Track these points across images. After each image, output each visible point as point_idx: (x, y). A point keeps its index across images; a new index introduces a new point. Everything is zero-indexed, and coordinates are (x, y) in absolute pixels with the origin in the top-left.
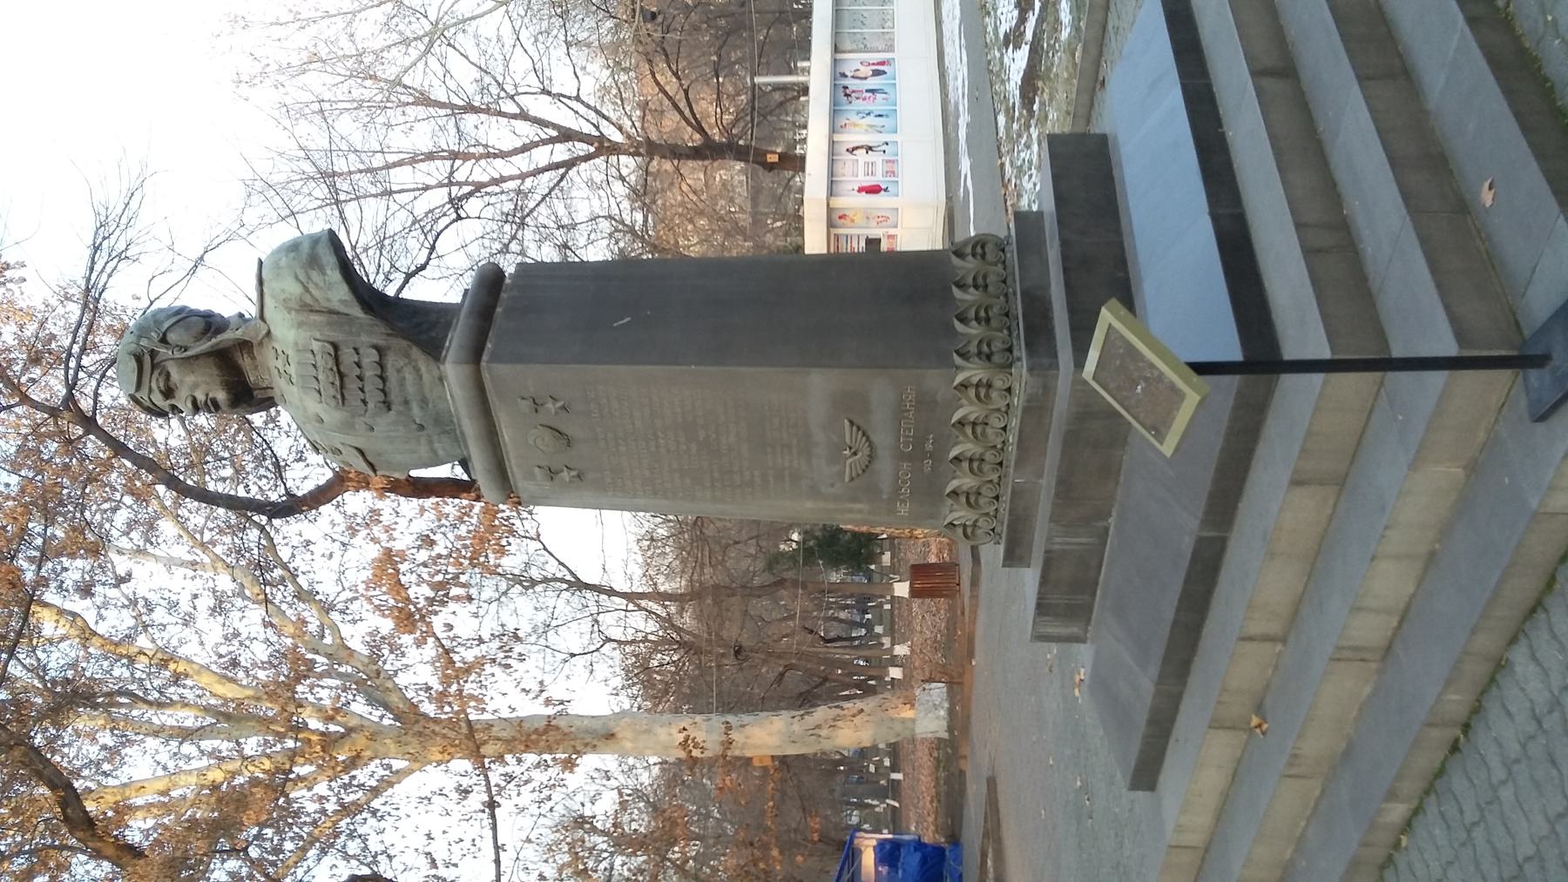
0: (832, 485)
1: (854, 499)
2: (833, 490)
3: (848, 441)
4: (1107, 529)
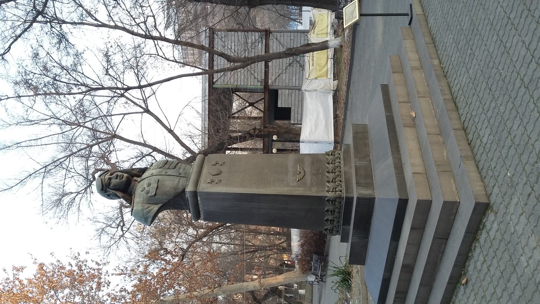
0: (293, 183)
1: (299, 187)
2: (293, 184)
3: (298, 170)
4: (370, 160)
